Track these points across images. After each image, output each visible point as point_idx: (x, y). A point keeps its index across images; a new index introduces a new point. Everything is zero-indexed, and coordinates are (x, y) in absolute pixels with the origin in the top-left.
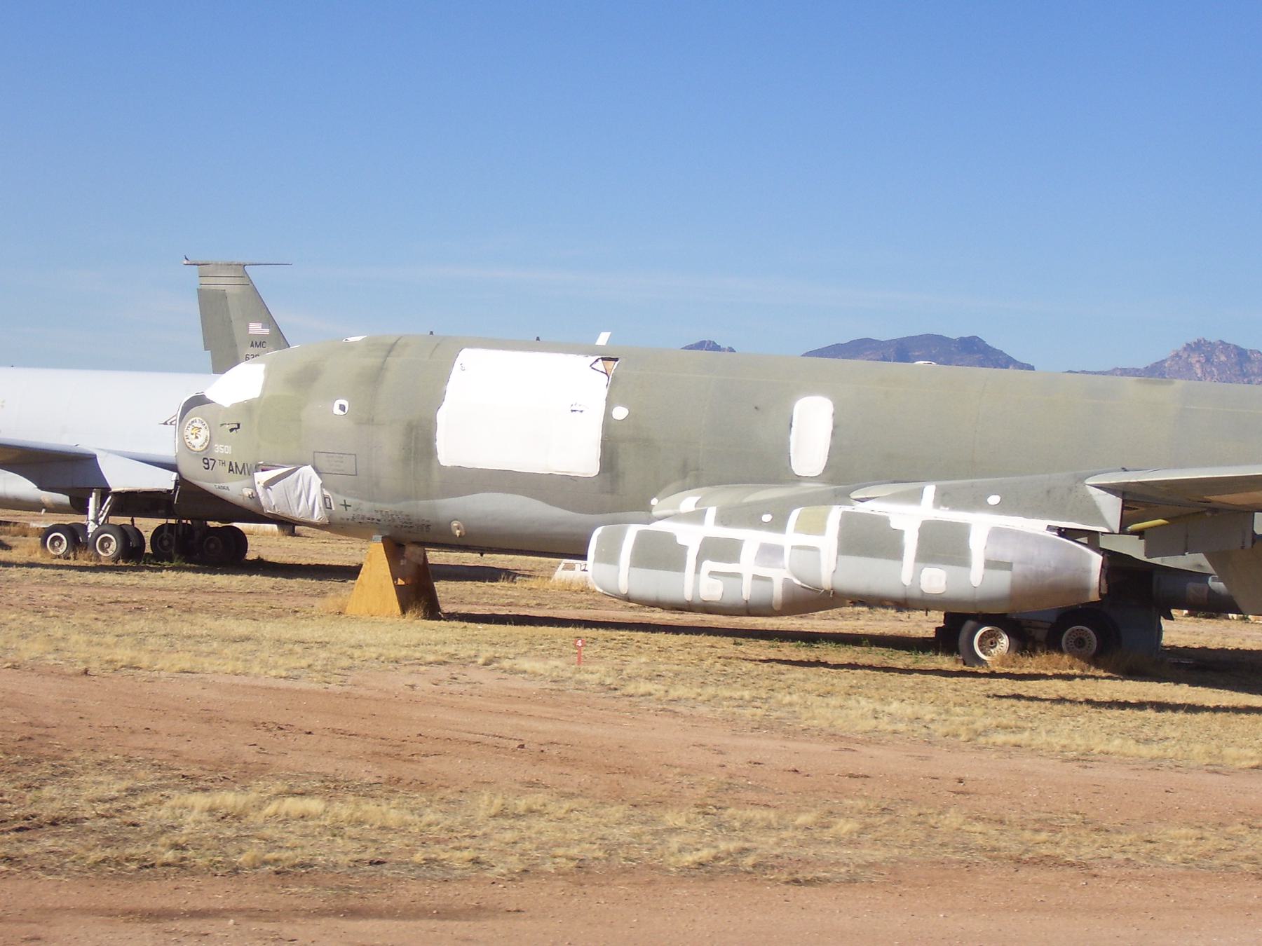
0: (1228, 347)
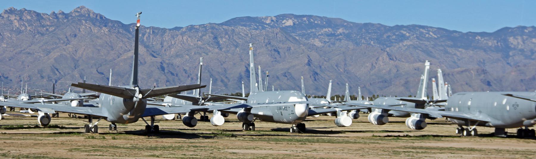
0: (30, 12)
